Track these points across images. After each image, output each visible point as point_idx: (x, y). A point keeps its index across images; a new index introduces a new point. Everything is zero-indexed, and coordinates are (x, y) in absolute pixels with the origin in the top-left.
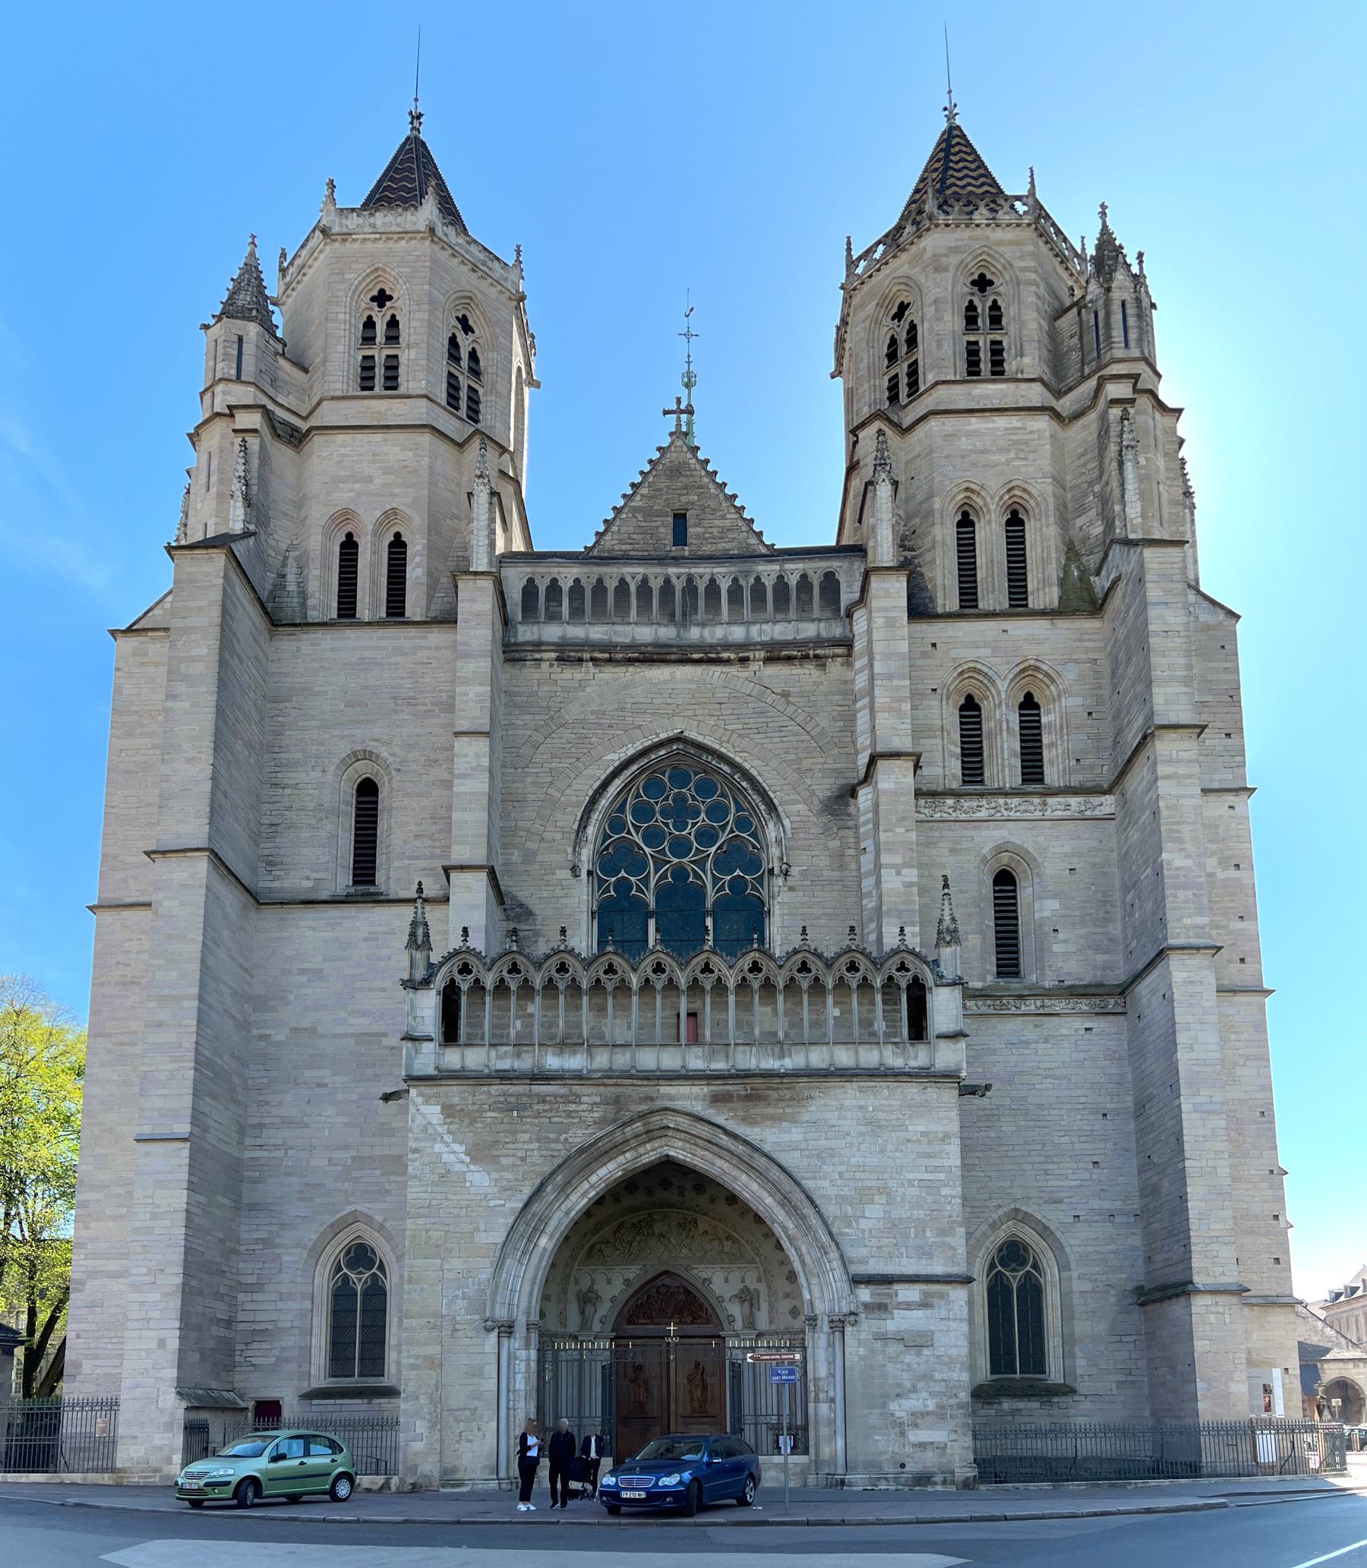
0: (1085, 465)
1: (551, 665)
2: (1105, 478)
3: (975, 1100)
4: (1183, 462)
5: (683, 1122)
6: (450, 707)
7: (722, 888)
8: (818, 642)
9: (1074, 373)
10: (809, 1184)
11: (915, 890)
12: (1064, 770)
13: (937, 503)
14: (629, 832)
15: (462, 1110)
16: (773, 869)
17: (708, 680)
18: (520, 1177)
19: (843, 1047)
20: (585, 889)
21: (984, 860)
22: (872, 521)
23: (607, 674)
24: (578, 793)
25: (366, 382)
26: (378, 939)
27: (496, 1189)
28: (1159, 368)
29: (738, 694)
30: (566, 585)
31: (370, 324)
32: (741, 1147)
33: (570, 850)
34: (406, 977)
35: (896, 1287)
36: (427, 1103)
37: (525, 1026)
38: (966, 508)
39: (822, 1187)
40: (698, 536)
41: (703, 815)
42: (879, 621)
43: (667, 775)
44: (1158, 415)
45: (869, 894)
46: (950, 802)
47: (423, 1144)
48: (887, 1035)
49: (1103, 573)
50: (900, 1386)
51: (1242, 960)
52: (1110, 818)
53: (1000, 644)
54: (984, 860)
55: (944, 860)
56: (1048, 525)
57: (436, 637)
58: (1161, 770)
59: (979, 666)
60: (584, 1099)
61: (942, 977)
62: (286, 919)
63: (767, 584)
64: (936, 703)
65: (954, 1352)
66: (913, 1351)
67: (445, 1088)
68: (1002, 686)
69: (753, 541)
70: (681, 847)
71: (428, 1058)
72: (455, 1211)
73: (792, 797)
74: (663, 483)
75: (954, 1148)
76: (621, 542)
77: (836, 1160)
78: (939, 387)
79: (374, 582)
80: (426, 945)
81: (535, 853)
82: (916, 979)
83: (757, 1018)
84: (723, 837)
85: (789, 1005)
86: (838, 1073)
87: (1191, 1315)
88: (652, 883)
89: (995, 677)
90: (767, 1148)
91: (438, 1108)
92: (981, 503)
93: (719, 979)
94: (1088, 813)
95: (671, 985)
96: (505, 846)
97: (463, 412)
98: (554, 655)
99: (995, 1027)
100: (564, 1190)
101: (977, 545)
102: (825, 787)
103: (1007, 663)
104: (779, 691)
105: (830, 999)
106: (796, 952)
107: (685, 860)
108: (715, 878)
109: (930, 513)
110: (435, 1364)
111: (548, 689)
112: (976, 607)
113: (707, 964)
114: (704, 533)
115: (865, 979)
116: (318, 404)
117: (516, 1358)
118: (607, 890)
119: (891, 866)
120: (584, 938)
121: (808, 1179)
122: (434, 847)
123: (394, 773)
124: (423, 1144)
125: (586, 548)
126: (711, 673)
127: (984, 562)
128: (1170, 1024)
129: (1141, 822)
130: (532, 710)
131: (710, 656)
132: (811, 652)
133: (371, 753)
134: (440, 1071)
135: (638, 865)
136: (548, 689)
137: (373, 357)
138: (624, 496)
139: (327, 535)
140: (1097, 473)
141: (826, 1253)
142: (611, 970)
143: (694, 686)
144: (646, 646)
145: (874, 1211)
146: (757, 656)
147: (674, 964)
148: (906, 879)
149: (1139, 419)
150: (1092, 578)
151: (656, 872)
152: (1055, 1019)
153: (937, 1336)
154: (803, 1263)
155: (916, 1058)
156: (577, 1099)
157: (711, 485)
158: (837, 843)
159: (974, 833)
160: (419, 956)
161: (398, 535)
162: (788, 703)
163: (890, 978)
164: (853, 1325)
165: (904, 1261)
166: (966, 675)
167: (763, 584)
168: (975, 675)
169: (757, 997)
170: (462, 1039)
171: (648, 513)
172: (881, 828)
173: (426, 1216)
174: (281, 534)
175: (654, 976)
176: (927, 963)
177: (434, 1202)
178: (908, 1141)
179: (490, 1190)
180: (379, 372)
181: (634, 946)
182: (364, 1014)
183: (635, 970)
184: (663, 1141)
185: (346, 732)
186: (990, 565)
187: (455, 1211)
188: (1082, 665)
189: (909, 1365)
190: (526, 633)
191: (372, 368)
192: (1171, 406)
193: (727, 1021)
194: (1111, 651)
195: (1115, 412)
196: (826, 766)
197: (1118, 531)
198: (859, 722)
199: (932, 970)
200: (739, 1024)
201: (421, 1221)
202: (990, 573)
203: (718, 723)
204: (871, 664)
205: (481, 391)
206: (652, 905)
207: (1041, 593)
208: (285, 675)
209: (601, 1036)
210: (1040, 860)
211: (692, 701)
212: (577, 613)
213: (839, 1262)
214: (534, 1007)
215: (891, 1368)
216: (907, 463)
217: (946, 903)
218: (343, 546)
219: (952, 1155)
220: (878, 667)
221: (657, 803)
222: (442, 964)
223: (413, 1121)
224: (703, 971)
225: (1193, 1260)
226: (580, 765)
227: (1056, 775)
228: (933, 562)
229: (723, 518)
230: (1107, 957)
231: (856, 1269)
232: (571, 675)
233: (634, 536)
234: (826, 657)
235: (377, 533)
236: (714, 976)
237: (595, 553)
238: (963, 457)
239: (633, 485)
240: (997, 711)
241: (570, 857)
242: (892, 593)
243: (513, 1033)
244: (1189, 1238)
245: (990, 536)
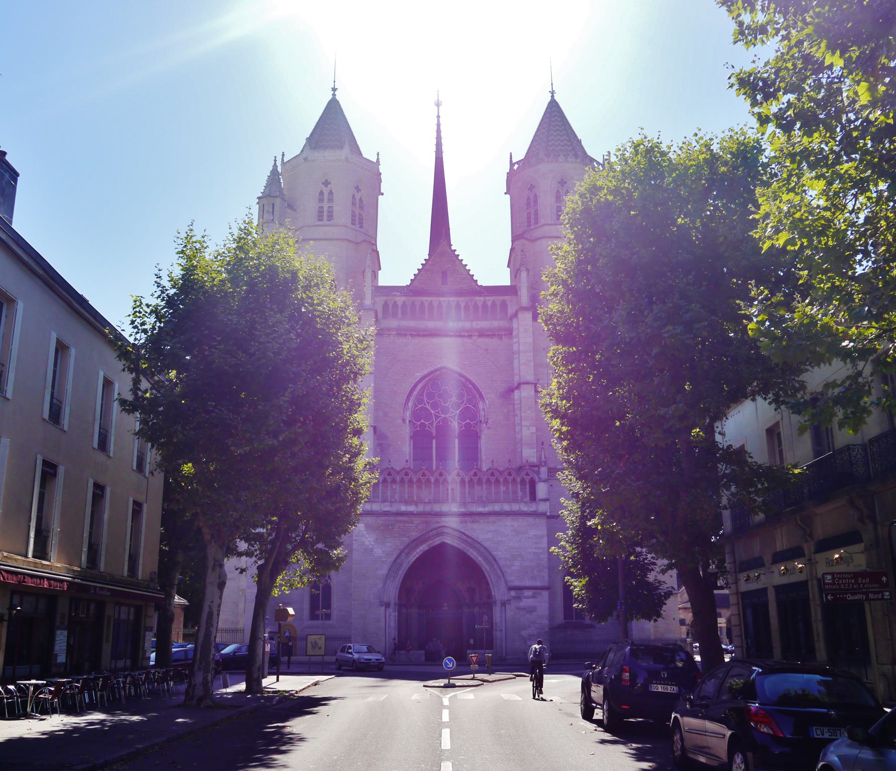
11: (535, 435)
14: (425, 404)
20: (408, 428)
23: (417, 340)
25: (320, 217)
30: (400, 304)
31: (321, 193)
33: (402, 412)
35: (524, 591)
69: (473, 284)
98: (395, 333)
104: (484, 348)
119: (526, 426)
120: (408, 447)
137: (323, 207)
151: (436, 420)
180: (325, 213)
190: (385, 323)
191: (323, 212)
234: (502, 335)
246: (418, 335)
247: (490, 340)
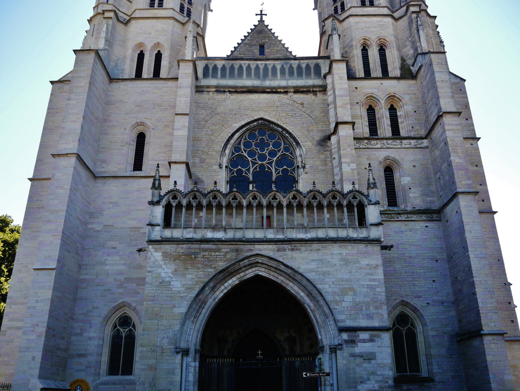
0: (405, 32)
1: (213, 93)
2: (413, 36)
3: (387, 251)
4: (438, 33)
5: (265, 261)
6: (174, 107)
7: (279, 173)
8: (314, 86)
9: (398, 6)
10: (319, 286)
11: (356, 172)
12: (408, 131)
13: (354, 43)
14: (242, 152)
15: (171, 254)
16: (299, 166)
17: (273, 99)
18: (194, 283)
19: (332, 229)
20: (224, 173)
21: (380, 163)
22: (332, 47)
23: (235, 96)
26: (141, 191)
27: (184, 289)
28: (427, 3)
30: (220, 66)
32: (290, 271)
33: (219, 158)
34: (150, 200)
35: (358, 332)
36: (156, 251)
37: (199, 221)
38: (364, 45)
39: (325, 288)
40: (268, 52)
41: (271, 146)
42: (336, 77)
43: (257, 132)
44: (428, 18)
45: (337, 174)
46: (366, 141)
47: (153, 269)
48: (349, 225)
49: (415, 65)
50: (362, 378)
51: (483, 201)
52: (427, 147)
53: (380, 88)
54: (380, 163)
55: (365, 162)
56: (394, 50)
57: (170, 83)
58: (446, 127)
59: (373, 95)
60: (223, 250)
61: (371, 201)
62: (106, 183)
63: (294, 67)
64: (359, 107)
65: (385, 361)
66: (367, 361)
67: (164, 245)
68: (382, 102)
70: (262, 158)
71: (157, 233)
72: (165, 298)
73: (305, 140)
74: (256, 36)
75: (380, 271)
76: (240, 54)
77: (331, 276)
78: (352, 8)
79: (149, 66)
80: (159, 188)
81: (205, 160)
82: (360, 201)
83: (296, 218)
84: (279, 154)
85: (308, 213)
86: (330, 239)
87: (483, 344)
88: (251, 171)
89: (379, 99)
90: (301, 271)
91: (160, 254)
92: (370, 43)
93: (280, 202)
94: (418, 146)
95: (260, 206)
96: (193, 157)
97: (185, 15)
98: (214, 90)
99: (389, 226)
100: (213, 289)
101: (369, 57)
102: (318, 136)
103: (383, 94)
105: (325, 210)
106: (311, 191)
107: (264, 162)
108: (276, 170)
109: (352, 46)
110: (153, 368)
111: (212, 101)
112: (370, 76)
113: (275, 196)
115: (339, 202)
116: (134, 11)
117: (190, 366)
118: (233, 173)
119: (346, 163)
121: (319, 284)
122: (165, 157)
123: (152, 130)
124: (153, 269)
125: (227, 56)
126: (274, 96)
127: (372, 62)
128: (461, 222)
129: (440, 147)
130: (206, 109)
131: (274, 91)
132: (311, 90)
133: (143, 123)
134: (162, 238)
135: (245, 163)
136: (212, 101)
138: (242, 40)
139: (134, 51)
140: (409, 35)
141: (327, 318)
142: (235, 198)
145: (348, 298)
146: (291, 90)
147: (261, 196)
148: (352, 168)
149: (422, 18)
150: (411, 68)
151: (253, 167)
152: (413, 222)
153: (377, 354)
154: (317, 322)
155: (362, 233)
156: (219, 250)
157: (273, 37)
158: (323, 156)
159: (376, 153)
160: (156, 192)
161: (159, 51)
162: (303, 107)
163: (350, 202)
164: (340, 350)
165: (361, 321)
166: (369, 98)
167: (293, 67)
168: (372, 98)
169: (295, 209)
170: (172, 225)
171: (250, 45)
172: (341, 149)
173: (153, 300)
174: (117, 51)
175: (253, 201)
176: (365, 196)
177: (156, 294)
178: (361, 268)
179: (181, 289)
181: (245, 191)
182: (134, 219)
183: (245, 199)
184: (256, 268)
185: (135, 115)
186: (374, 63)
187: (165, 298)
188: (411, 95)
189: (366, 368)
190: (204, 82)
192: (432, 14)
193: (283, 219)
194: (421, 90)
195: (414, 16)
197: (419, 51)
198: (330, 113)
199: (366, 198)
200: (288, 220)
201: (150, 303)
202: (374, 65)
203: (277, 113)
204: (334, 92)
205: (192, 9)
206: (251, 179)
207: (393, 72)
208: (113, 96)
209: (230, 225)
210: (401, 162)
211: (267, 106)
212: (223, 76)
213: (333, 321)
214: (203, 213)
215: (358, 369)
216: (342, 31)
217: (370, 172)
218: (139, 54)
219: (380, 274)
220: (337, 93)
221: (253, 142)
222: (165, 195)
223: (149, 259)
224: (273, 199)
225: (482, 320)
226: (224, 128)
227: (405, 133)
228: (354, 61)
229: (278, 47)
230: (431, 199)
231: (341, 324)
232: (221, 97)
233: (245, 52)
234: (317, 91)
235: (152, 50)
236: (278, 201)
237: (231, 57)
239: (245, 36)
240: (381, 110)
241: (219, 161)
242: (340, 69)
243: (193, 224)
244: (479, 310)
245: (374, 54)
246: (236, 92)
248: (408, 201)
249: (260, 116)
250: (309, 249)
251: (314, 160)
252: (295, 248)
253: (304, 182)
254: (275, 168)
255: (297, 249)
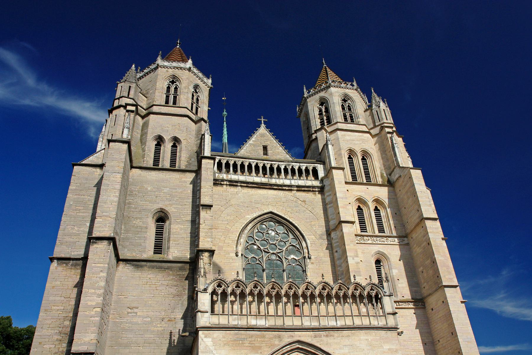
1: (227, 187)
14: (255, 242)
17: (279, 195)
23: (246, 191)
24: (237, 228)
29: (289, 200)
33: (235, 247)
88: (264, 259)
103: (370, 197)
114: (273, 153)
131: (280, 187)
143: (275, 196)
144: (259, 183)
162: (305, 204)
196: (319, 224)
232: (233, 189)
234: (316, 191)
238: (348, 141)
241: (235, 249)
247: (306, 195)
248: (397, 291)
249: (269, 210)
250: (341, 336)
251: (318, 252)
252: (329, 334)
253: (311, 271)
254: (285, 258)
255: (331, 336)
